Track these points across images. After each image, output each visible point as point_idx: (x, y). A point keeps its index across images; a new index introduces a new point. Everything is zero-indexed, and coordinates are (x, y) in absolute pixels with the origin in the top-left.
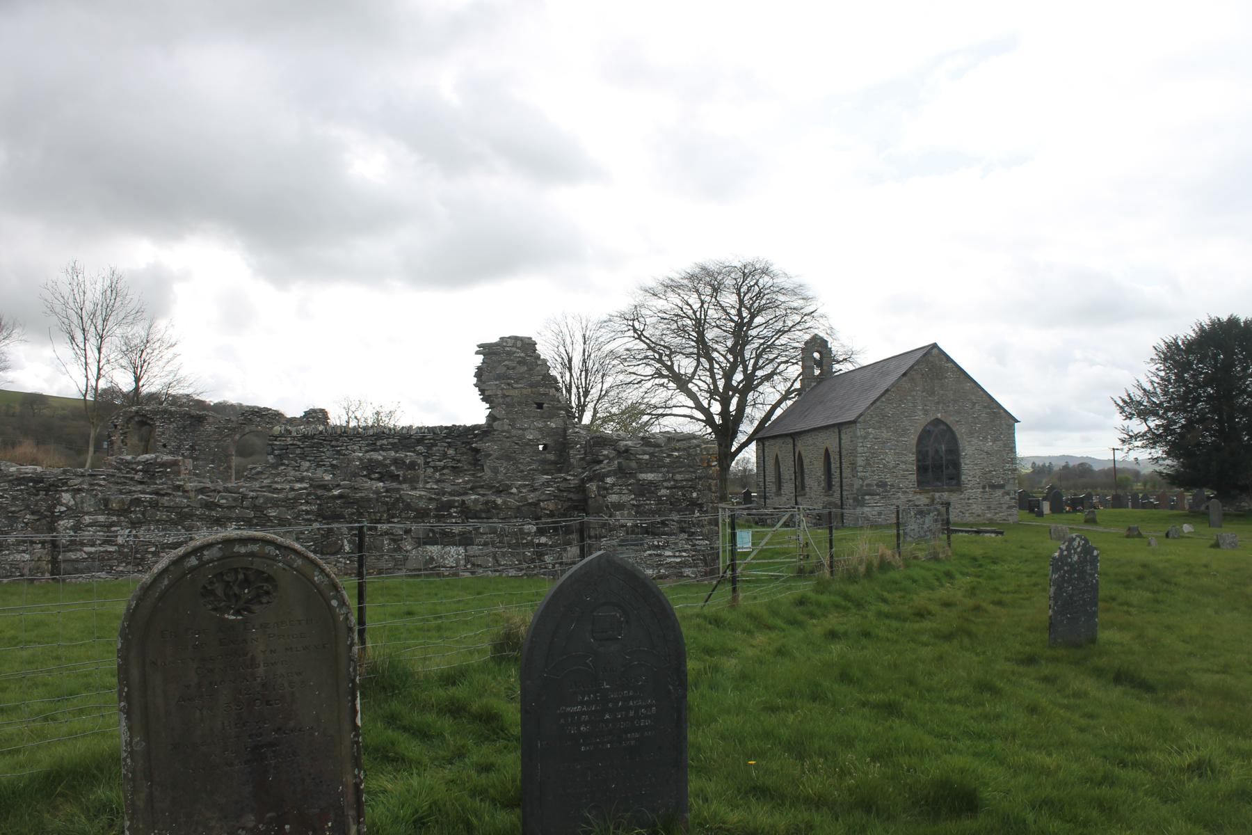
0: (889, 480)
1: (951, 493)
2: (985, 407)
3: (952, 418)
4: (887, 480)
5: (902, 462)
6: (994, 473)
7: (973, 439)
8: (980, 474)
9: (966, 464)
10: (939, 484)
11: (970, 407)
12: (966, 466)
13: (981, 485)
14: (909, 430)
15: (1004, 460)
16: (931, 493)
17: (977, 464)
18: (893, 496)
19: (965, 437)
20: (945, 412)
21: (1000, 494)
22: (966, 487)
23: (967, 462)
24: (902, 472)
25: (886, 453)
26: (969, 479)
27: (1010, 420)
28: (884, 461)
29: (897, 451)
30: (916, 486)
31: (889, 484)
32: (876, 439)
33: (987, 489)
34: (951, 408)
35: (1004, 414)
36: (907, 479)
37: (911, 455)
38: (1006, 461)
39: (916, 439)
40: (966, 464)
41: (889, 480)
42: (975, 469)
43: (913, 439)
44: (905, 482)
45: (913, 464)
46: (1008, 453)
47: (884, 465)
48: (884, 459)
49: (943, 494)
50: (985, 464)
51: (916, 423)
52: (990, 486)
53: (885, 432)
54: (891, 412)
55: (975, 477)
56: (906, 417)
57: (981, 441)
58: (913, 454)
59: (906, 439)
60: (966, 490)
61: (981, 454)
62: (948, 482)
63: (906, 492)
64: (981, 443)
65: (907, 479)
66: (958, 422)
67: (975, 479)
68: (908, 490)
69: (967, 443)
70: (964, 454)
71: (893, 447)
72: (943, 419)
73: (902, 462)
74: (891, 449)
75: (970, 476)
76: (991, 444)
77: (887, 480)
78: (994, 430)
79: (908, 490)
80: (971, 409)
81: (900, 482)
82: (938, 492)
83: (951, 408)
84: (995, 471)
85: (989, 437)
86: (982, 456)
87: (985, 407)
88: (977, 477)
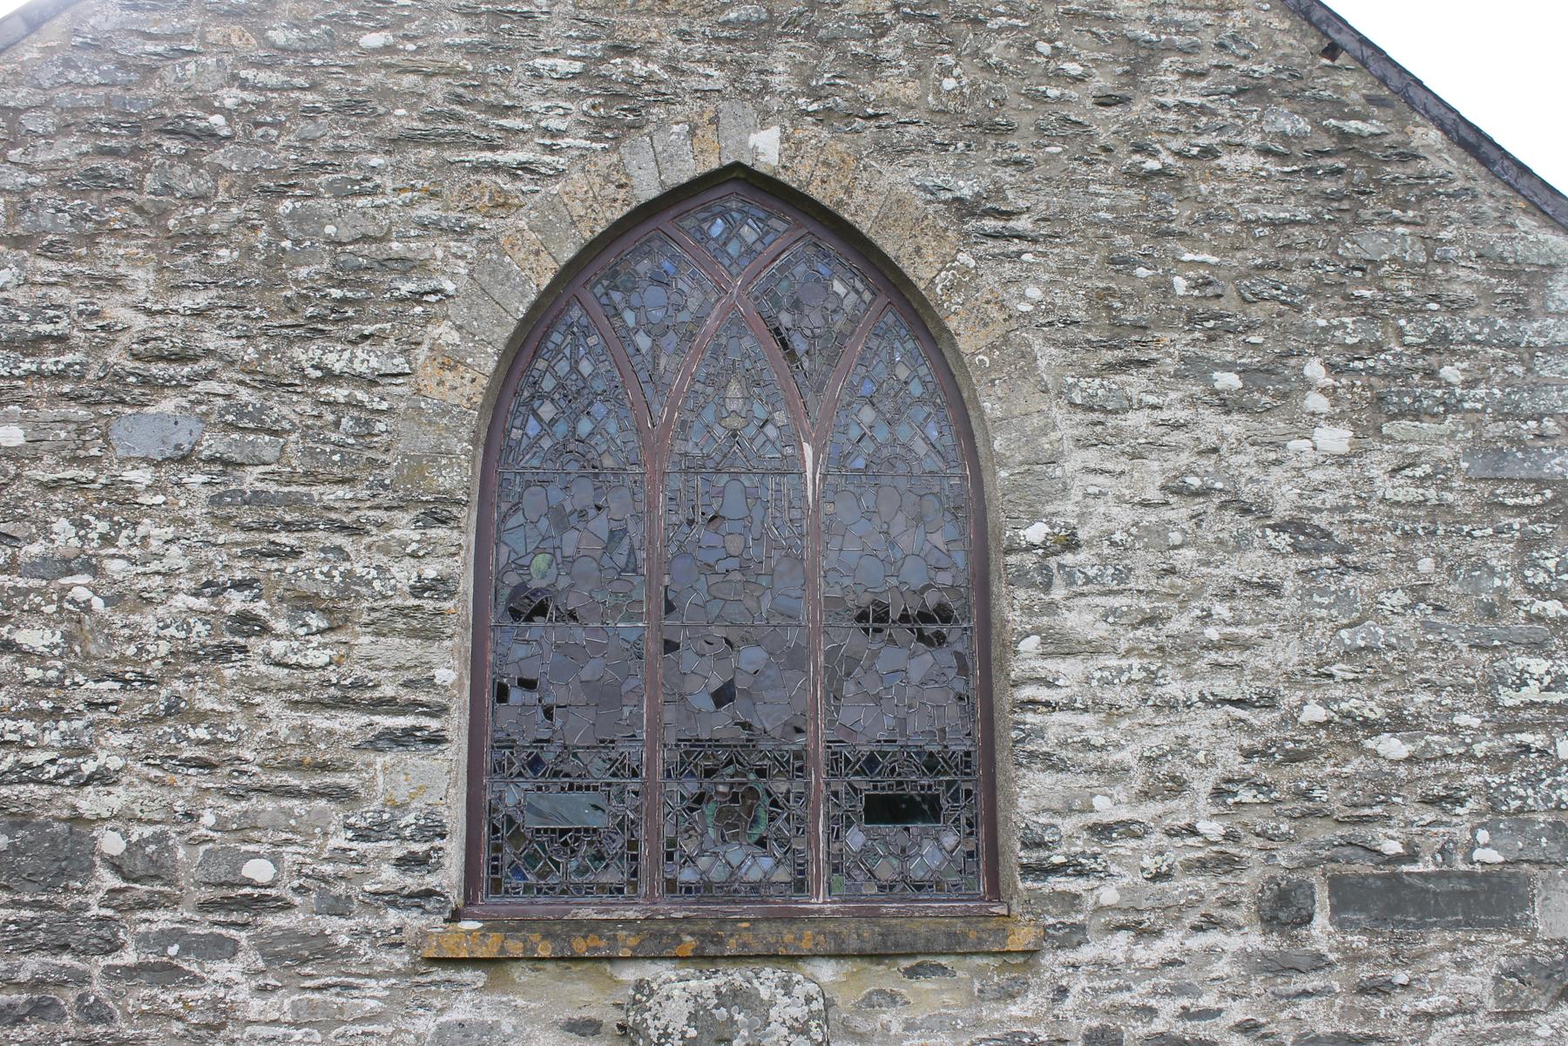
0: (117, 799)
1: (885, 977)
2: (1252, 91)
3: (898, 177)
4: (89, 802)
5: (303, 602)
6: (1393, 747)
7: (1135, 383)
8: (1232, 762)
9: (1060, 645)
10: (759, 867)
11: (1102, 82)
12: (1069, 670)
13: (1251, 879)
14: (407, 266)
15: (1490, 611)
16: (629, 974)
17: (1186, 649)
18: (141, 995)
19: (1047, 356)
20: (824, 117)
21: (1478, 983)
22: (1072, 900)
23: (1080, 621)
24: (282, 720)
25: (121, 499)
26: (1106, 808)
27: (1526, 223)
28: (80, 586)
29: (251, 479)
30: (449, 876)
31: (112, 843)
32: (35, 344)
33: (1321, 931)
34: (895, 85)
35: (1444, 160)
36: (343, 795)
37: (405, 529)
38: (1515, 621)
39: (488, 362)
40: (1060, 645)
41: (117, 799)
42: (1170, 705)
43: (450, 361)
44: (303, 832)
45: (429, 634)
46: (1528, 543)
47: (75, 618)
48: (94, 570)
49: (766, 982)
50: (1289, 653)
51: (502, 203)
52: (1347, 895)
53: (142, 279)
54: (230, 97)
55: (1177, 786)
56: (396, 143)
57: (1226, 404)
58: (435, 515)
59: (366, 360)
60: (1074, 936)
61: (1241, 544)
62: (855, 838)
63: (322, 950)
64: (1234, 426)
65: (343, 795)
66: (964, 209)
67: (1179, 811)
68: (339, 929)
69: (1067, 425)
70: (1036, 533)
71: (213, 443)
72: (803, 175)
73: (303, 602)
74: (184, 459)
75: (1116, 773)
76: (1335, 438)
77: (89, 802)
78: (1367, 310)
79: (339, 929)
80: (1105, 101)
81: (246, 828)
82: (703, 959)
83: (895, 85)
84: (1398, 723)
85: (1314, 369)
86: (1251, 564)
87: (1252, 91)
88: (1203, 785)
